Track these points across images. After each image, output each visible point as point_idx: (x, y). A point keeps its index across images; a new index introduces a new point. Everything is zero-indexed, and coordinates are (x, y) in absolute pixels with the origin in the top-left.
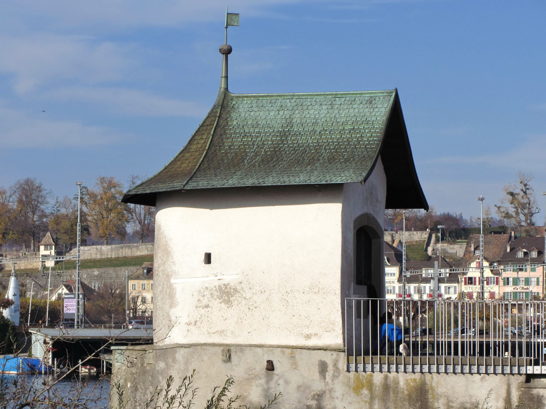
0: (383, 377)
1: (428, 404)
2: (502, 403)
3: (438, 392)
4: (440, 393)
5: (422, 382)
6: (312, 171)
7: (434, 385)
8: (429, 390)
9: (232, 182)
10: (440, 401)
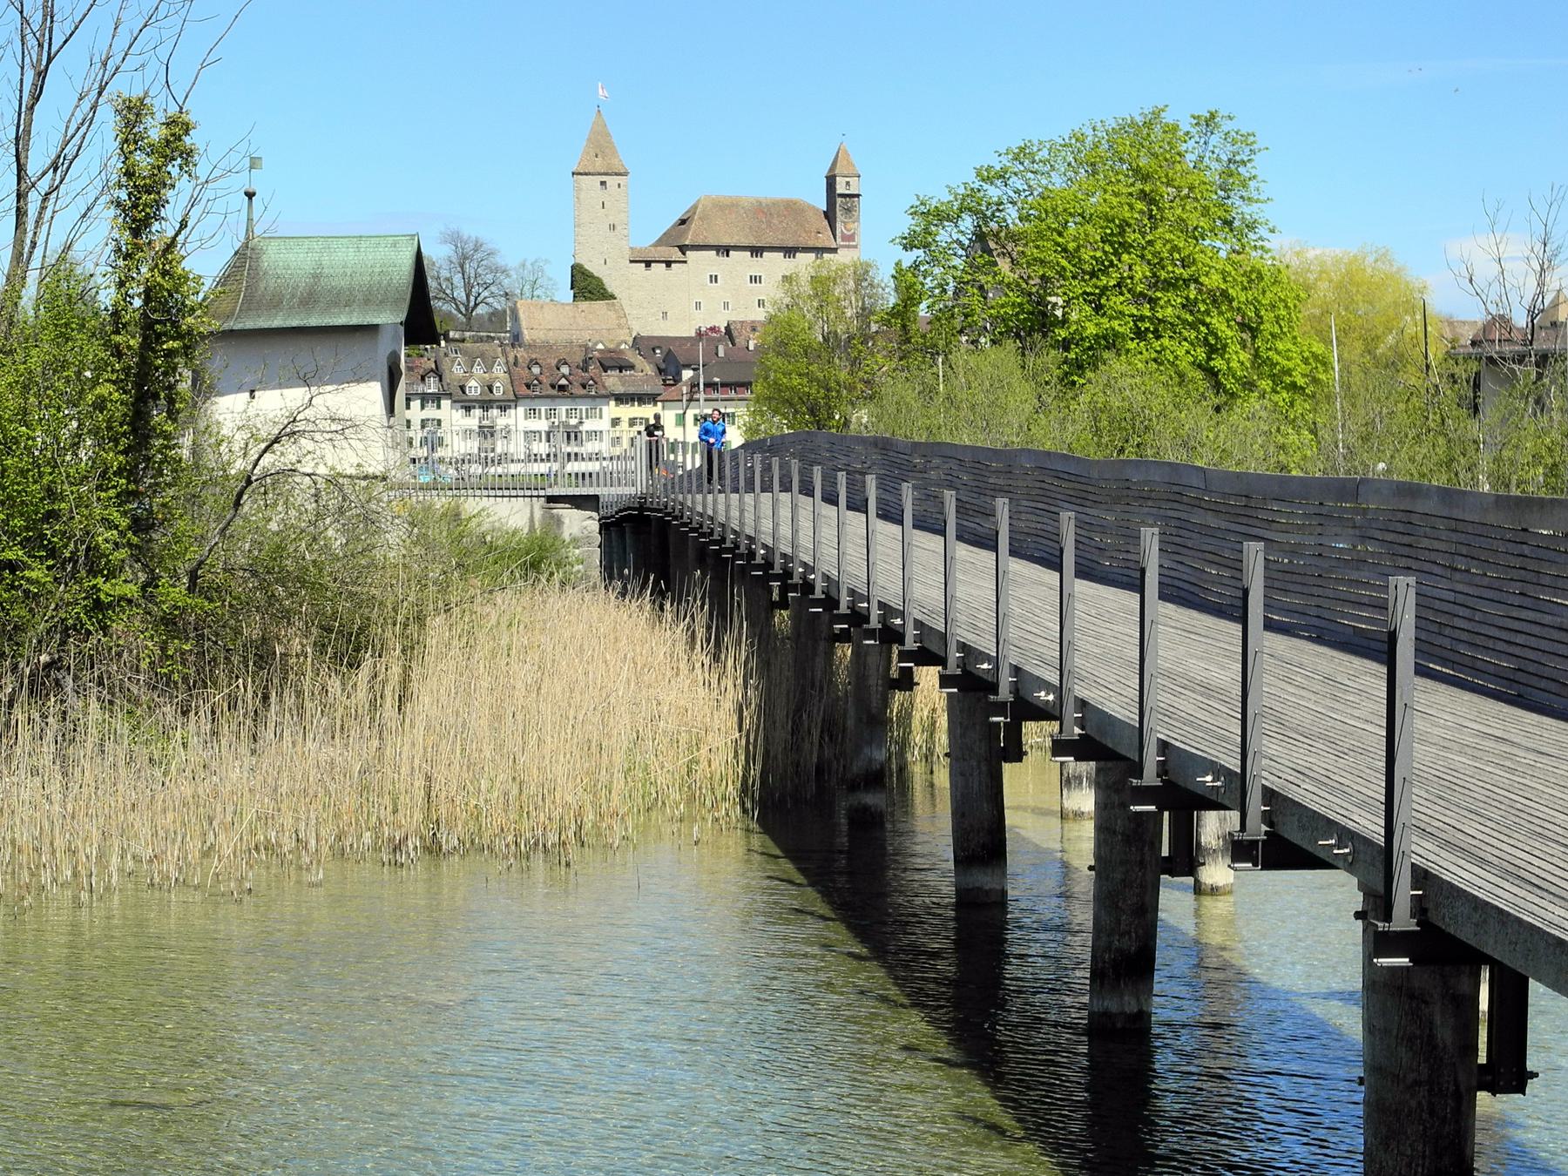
6: (351, 312)
9: (277, 323)
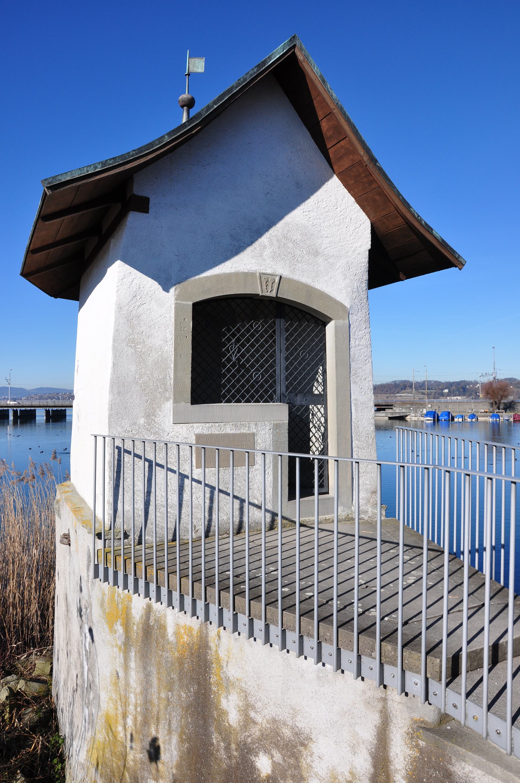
0: (145, 607)
1: (210, 695)
2: (365, 760)
3: (229, 674)
4: (231, 678)
5: (201, 637)
7: (222, 654)
8: (212, 663)
10: (230, 697)
